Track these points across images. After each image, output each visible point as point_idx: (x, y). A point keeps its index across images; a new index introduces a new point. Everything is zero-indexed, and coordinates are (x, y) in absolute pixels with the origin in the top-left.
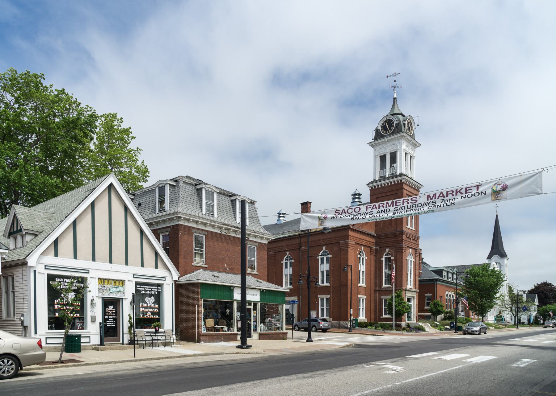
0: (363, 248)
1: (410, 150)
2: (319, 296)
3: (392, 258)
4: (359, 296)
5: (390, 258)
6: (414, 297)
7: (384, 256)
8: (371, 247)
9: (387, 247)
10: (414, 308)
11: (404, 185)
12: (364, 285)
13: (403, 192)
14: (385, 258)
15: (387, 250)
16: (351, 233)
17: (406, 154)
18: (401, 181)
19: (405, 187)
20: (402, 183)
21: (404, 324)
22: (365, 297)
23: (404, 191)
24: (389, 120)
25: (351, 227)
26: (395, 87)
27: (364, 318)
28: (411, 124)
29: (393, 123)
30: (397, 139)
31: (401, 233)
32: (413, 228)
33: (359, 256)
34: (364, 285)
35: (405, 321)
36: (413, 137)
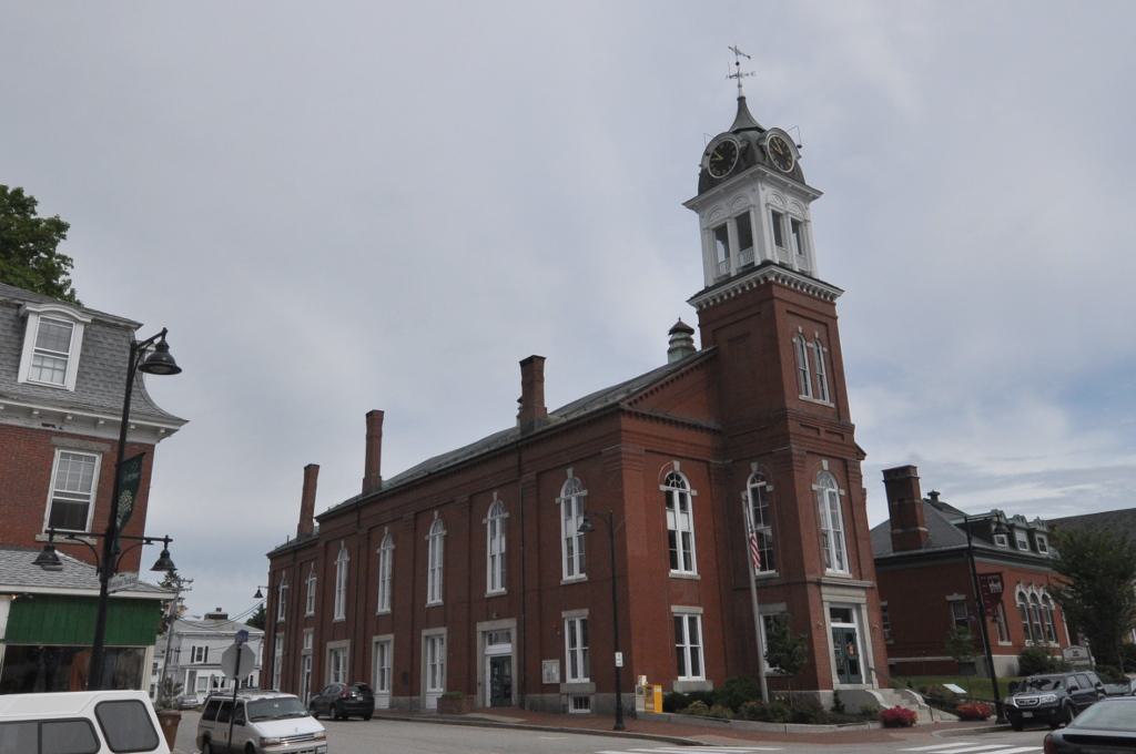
0: (677, 465)
1: (789, 205)
2: (564, 614)
3: (769, 488)
4: (675, 609)
5: (763, 488)
6: (858, 606)
7: (749, 486)
8: (707, 462)
9: (752, 459)
10: (863, 641)
11: (774, 288)
12: (693, 573)
13: (773, 307)
14: (754, 491)
15: (754, 466)
16: (626, 423)
17: (777, 216)
18: (766, 279)
19: (776, 292)
20: (769, 284)
21: (825, 697)
22: (701, 610)
23: (777, 304)
24: (725, 143)
25: (625, 406)
26: (738, 75)
27: (702, 678)
28: (785, 148)
29: (734, 148)
30: (745, 183)
31: (782, 416)
32: (827, 402)
33: (663, 488)
34: (693, 573)
35: (830, 686)
36: (797, 175)
